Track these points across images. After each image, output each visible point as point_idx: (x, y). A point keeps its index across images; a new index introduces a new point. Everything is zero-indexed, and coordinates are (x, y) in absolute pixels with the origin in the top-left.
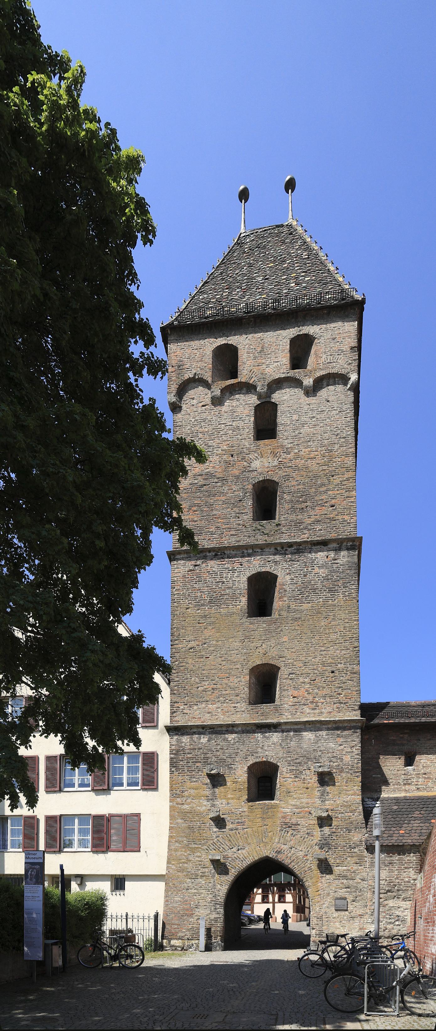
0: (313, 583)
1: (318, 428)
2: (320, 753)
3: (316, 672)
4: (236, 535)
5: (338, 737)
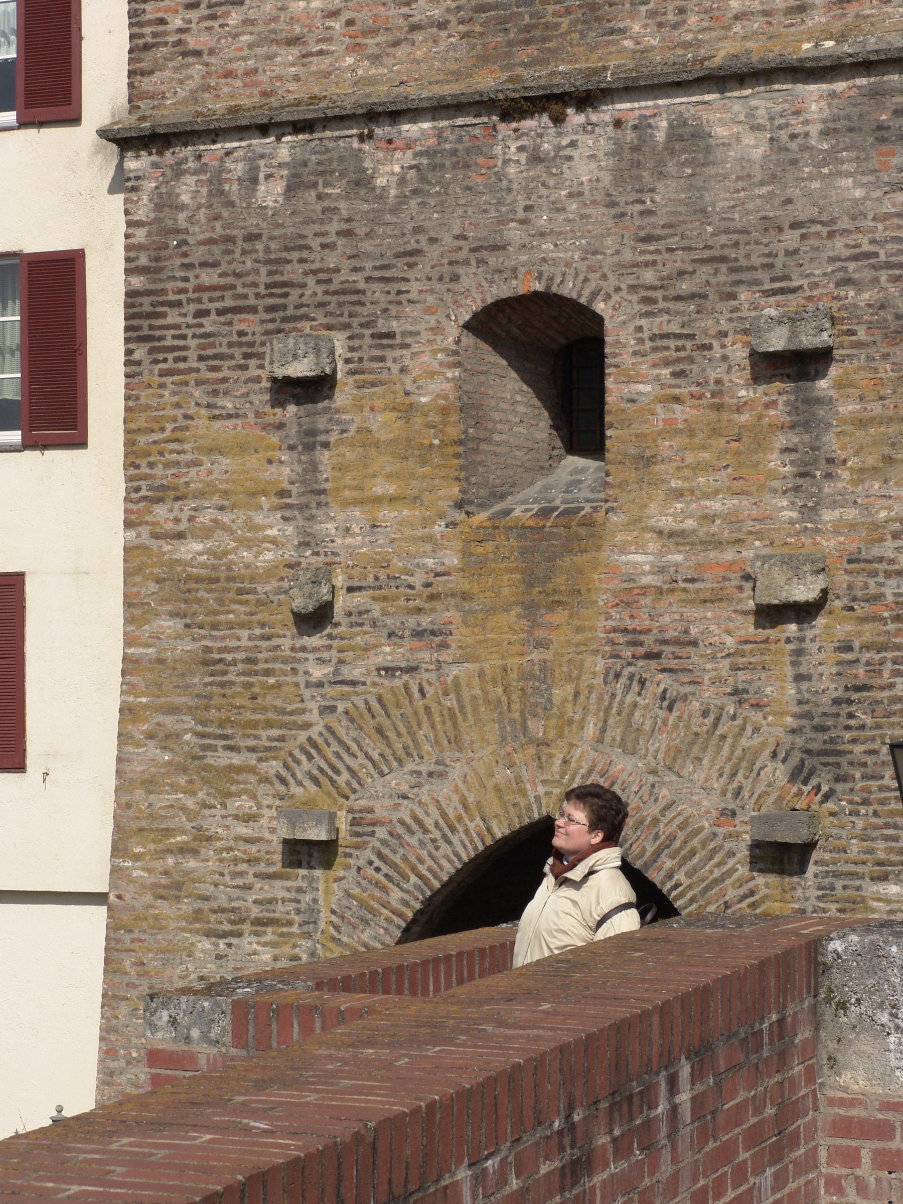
2: (791, 238)
5: (882, 140)
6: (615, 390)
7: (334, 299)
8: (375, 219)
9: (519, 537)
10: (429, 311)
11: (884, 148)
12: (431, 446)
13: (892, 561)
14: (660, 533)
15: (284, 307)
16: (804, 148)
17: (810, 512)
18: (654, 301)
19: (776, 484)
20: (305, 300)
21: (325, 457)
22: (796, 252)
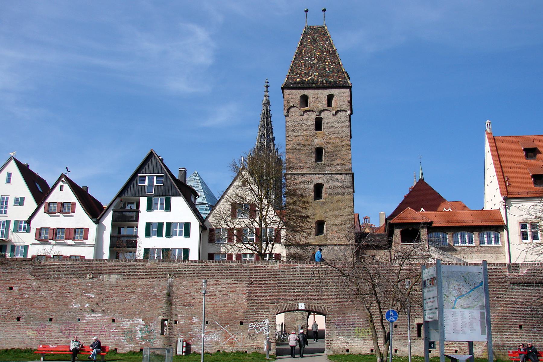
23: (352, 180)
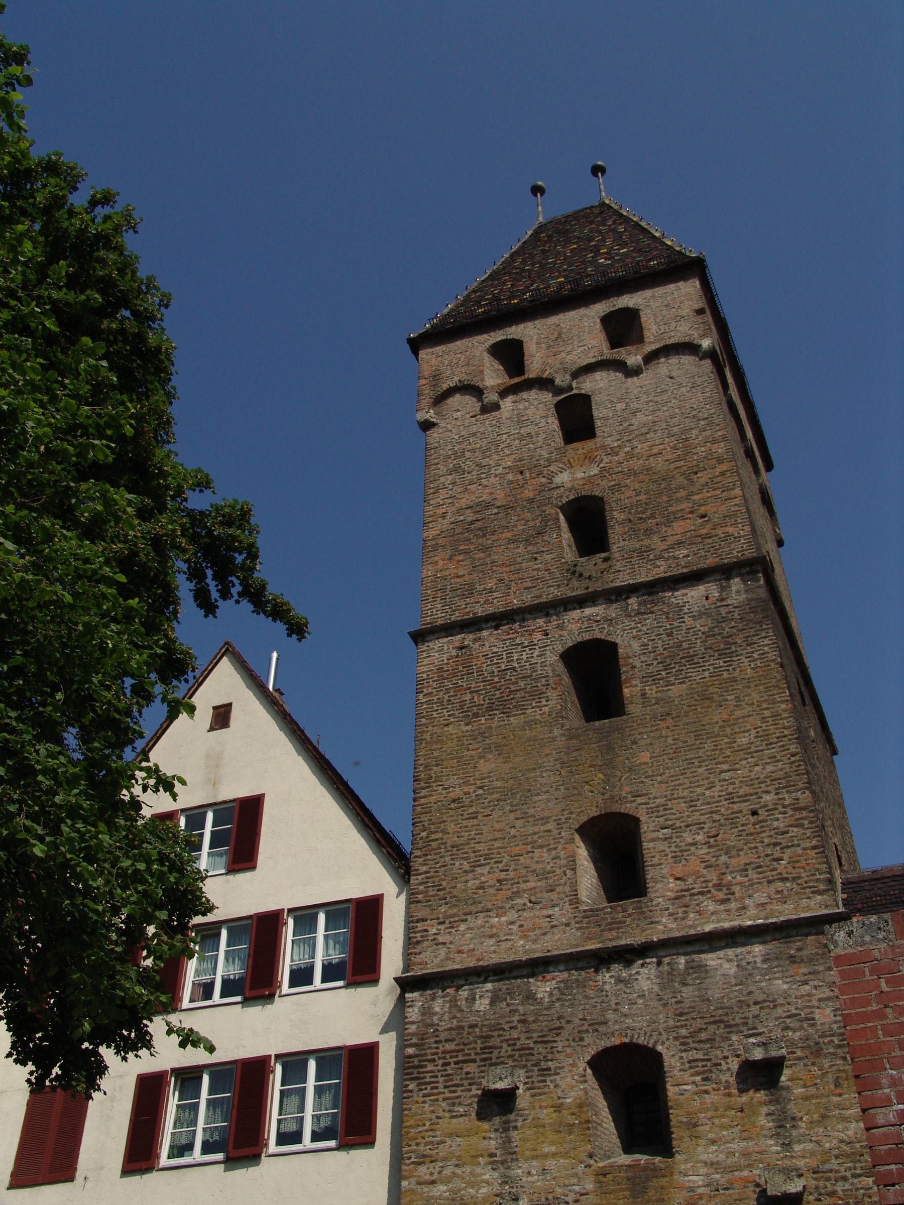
0: (685, 645)
1: (659, 413)
2: (755, 1009)
3: (716, 817)
4: (534, 587)
5: (793, 962)
6: (672, 1091)
7: (517, 1053)
8: (538, 1014)
9: (626, 1171)
10: (568, 1056)
11: (795, 966)
12: (574, 1124)
13: (837, 1171)
14: (706, 1163)
15: (491, 1059)
16: (755, 968)
17: (787, 1146)
18: (688, 1044)
19: (765, 1132)
20: (502, 1054)
21: (514, 1134)
22: (758, 1016)
23: (763, 593)
